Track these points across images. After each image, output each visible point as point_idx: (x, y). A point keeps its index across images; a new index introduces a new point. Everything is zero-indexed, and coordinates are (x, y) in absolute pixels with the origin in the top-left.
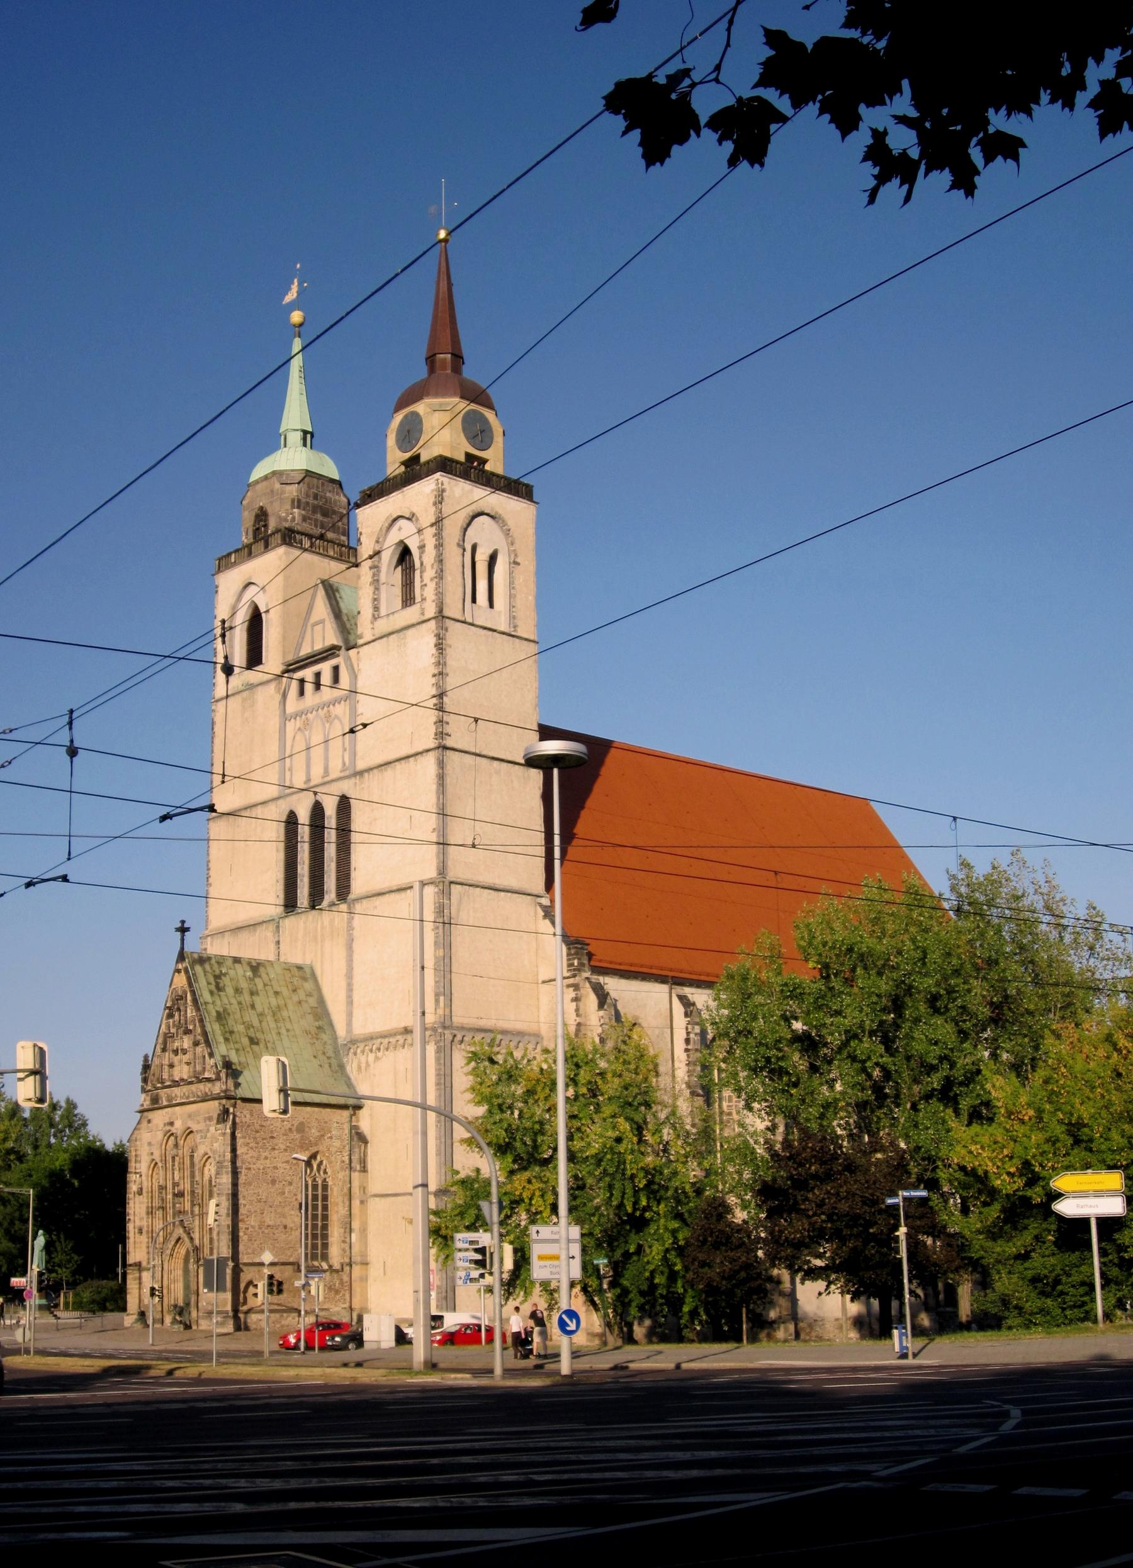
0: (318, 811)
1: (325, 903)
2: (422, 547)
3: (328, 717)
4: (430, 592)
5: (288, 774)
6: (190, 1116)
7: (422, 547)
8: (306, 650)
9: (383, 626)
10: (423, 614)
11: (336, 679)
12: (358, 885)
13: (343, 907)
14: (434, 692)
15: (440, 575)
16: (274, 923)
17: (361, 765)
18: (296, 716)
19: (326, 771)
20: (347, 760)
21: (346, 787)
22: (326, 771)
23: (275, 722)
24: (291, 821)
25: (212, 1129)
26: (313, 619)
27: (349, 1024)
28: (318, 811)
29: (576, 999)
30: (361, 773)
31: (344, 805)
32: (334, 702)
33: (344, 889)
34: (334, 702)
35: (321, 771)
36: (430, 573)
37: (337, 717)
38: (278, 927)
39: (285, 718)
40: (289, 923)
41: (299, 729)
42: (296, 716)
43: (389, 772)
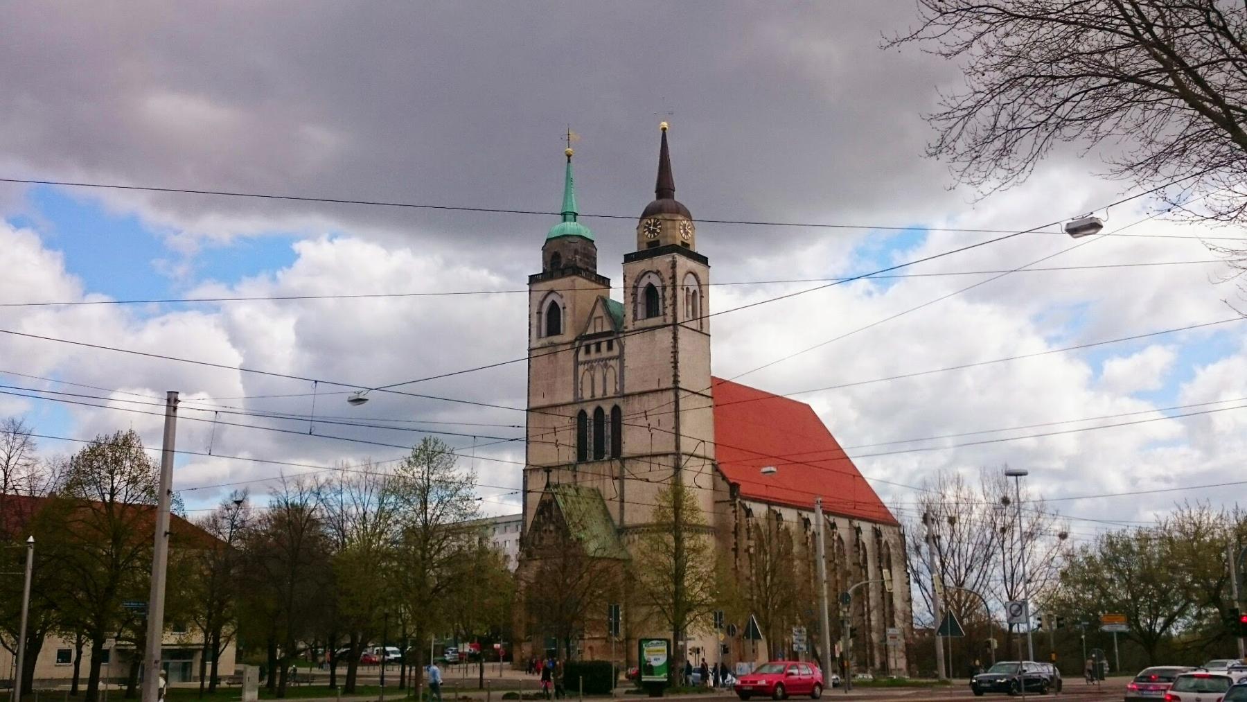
0: (599, 411)
1: (605, 458)
2: (664, 288)
3: (606, 366)
4: (669, 311)
8: (590, 331)
9: (639, 324)
11: (610, 348)
12: (627, 450)
13: (617, 463)
15: (674, 304)
16: (572, 467)
17: (627, 391)
18: (585, 363)
19: (605, 391)
22: (605, 391)
23: (571, 364)
24: (582, 414)
26: (596, 314)
27: (622, 520)
28: (599, 411)
29: (735, 512)
30: (628, 395)
31: (616, 410)
32: (610, 359)
34: (610, 359)
36: (668, 302)
38: (575, 470)
39: (577, 364)
40: (582, 467)
42: (585, 363)
43: (645, 398)
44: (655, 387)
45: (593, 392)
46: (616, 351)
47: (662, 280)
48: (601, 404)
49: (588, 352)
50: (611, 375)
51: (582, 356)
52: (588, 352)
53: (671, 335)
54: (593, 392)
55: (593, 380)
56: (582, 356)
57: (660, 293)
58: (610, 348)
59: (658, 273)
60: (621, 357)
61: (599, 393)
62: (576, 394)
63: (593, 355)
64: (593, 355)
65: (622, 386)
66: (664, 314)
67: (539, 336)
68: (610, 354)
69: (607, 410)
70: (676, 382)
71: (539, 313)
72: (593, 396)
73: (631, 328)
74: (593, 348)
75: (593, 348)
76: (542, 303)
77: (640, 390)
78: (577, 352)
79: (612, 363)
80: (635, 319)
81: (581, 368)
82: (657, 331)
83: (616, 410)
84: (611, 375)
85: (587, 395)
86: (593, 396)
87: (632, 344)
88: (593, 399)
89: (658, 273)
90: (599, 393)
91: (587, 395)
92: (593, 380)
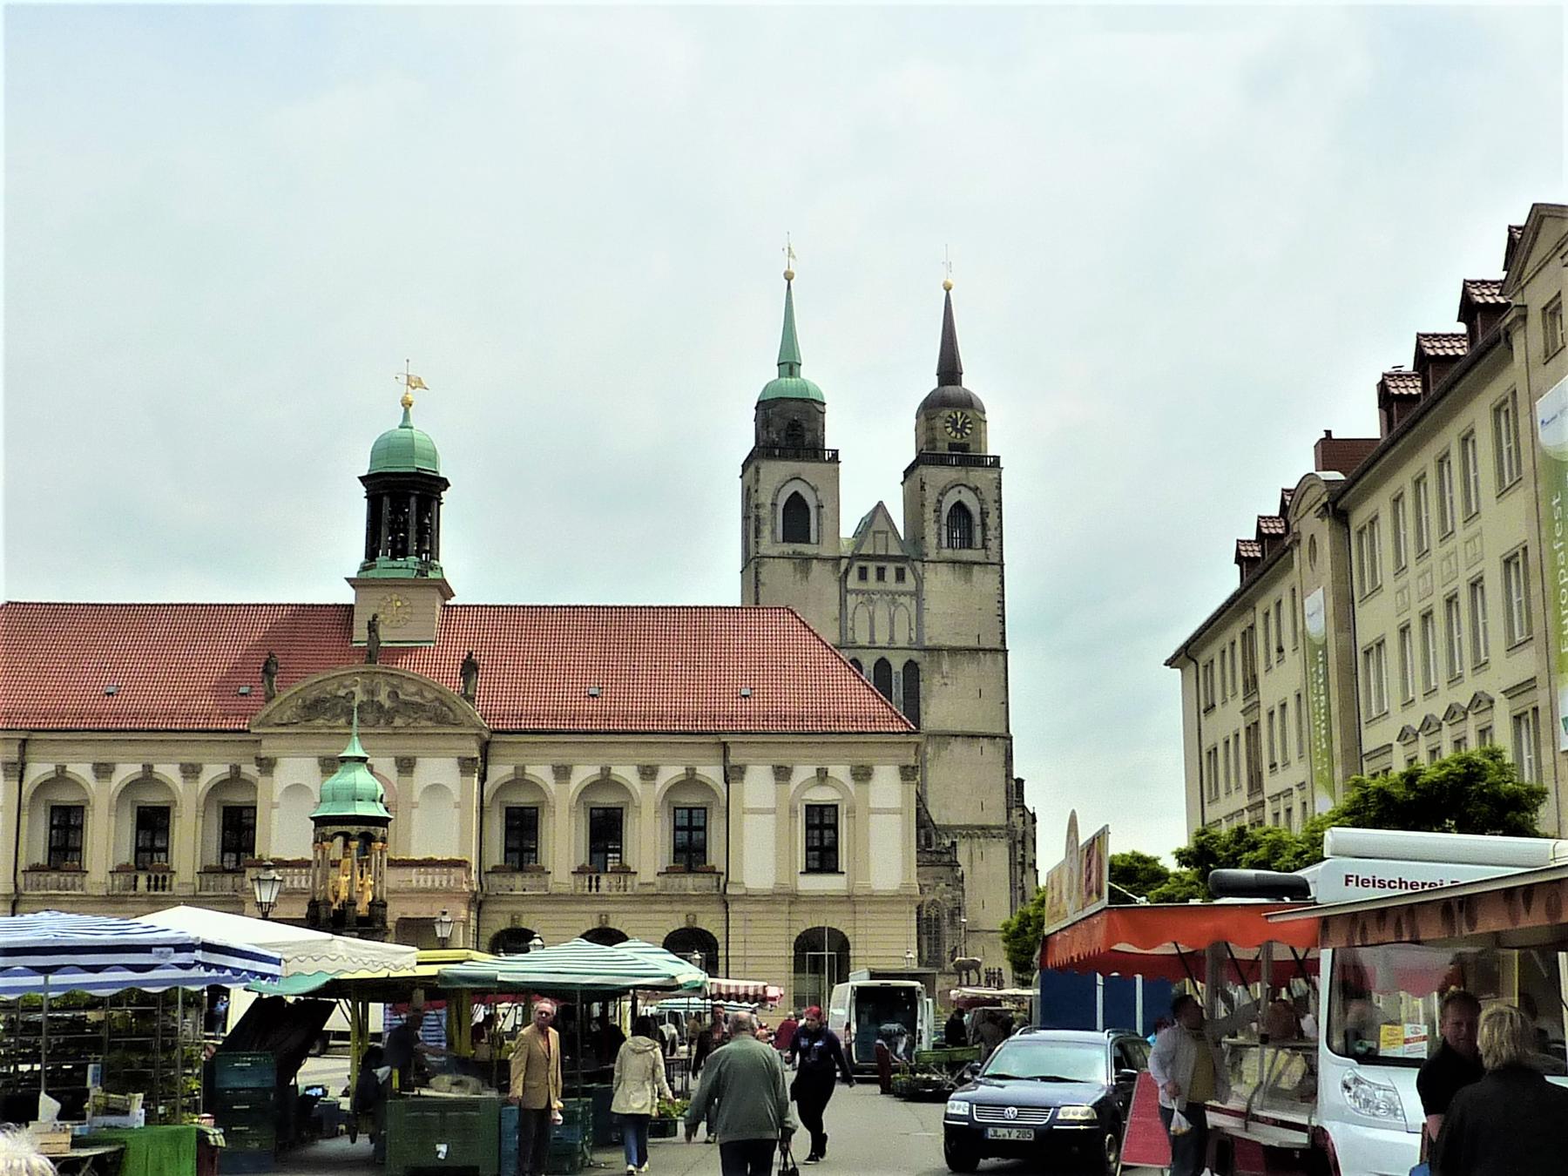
3: (894, 602)
7: (984, 514)
9: (947, 553)
11: (900, 576)
18: (857, 592)
19: (892, 638)
20: (913, 636)
21: (915, 656)
22: (892, 638)
23: (833, 590)
25: (942, 885)
26: (874, 528)
31: (911, 668)
39: (844, 592)
42: (857, 592)
44: (973, 643)
45: (872, 635)
46: (910, 583)
47: (982, 501)
48: (886, 654)
50: (902, 617)
51: (853, 582)
54: (872, 635)
55: (872, 619)
56: (853, 582)
57: (977, 519)
58: (900, 576)
59: (975, 490)
60: (917, 595)
62: (842, 631)
63: (872, 582)
64: (872, 582)
66: (985, 547)
68: (901, 587)
69: (897, 664)
70: (1003, 641)
71: (774, 505)
72: (872, 641)
73: (932, 555)
74: (872, 574)
75: (872, 574)
78: (847, 572)
79: (902, 599)
81: (851, 599)
82: (976, 567)
86: (872, 641)
87: (938, 581)
88: (872, 647)
89: (975, 490)
91: (863, 639)
92: (872, 619)
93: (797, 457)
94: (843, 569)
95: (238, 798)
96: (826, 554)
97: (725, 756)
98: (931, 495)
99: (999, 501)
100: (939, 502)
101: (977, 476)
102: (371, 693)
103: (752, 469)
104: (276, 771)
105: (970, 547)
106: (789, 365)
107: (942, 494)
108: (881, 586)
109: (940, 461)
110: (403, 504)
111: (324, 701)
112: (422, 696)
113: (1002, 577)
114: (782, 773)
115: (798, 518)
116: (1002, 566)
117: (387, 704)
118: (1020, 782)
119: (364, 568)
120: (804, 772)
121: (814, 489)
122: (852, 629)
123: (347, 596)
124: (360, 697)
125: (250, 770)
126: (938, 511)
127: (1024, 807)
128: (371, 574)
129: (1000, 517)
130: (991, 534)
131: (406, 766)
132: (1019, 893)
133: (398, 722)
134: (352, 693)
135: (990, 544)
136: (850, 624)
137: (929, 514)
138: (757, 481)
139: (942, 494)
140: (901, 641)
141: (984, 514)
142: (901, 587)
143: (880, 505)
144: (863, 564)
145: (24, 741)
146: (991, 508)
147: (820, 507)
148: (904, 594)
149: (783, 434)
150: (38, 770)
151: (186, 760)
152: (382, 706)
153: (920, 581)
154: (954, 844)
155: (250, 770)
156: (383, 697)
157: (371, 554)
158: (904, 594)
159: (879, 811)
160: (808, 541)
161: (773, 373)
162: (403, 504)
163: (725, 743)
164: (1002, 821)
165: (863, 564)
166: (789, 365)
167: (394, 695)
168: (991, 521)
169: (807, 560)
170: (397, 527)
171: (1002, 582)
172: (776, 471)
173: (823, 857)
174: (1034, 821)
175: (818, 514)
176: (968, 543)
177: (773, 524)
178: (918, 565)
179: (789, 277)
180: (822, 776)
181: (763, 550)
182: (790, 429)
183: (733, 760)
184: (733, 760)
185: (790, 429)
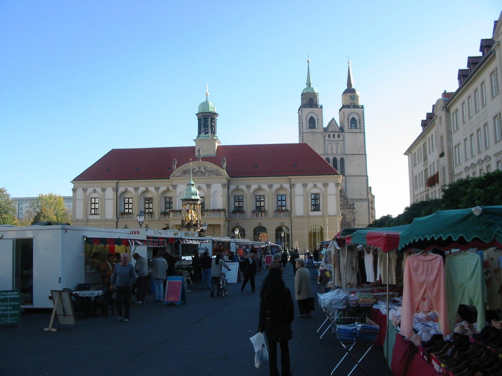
0: (335, 160)
5: (326, 151)
6: (344, 211)
7: (360, 120)
10: (361, 131)
11: (339, 136)
12: (347, 173)
14: (364, 145)
17: (346, 153)
18: (328, 141)
19: (337, 152)
21: (343, 156)
22: (337, 152)
23: (322, 141)
25: (351, 214)
33: (343, 173)
35: (336, 152)
37: (339, 143)
39: (325, 140)
41: (329, 143)
42: (328, 141)
47: (359, 117)
49: (329, 136)
51: (327, 138)
52: (329, 136)
53: (364, 136)
57: (358, 121)
58: (339, 136)
59: (357, 114)
60: (343, 141)
61: (334, 152)
62: (325, 151)
65: (344, 151)
66: (360, 128)
67: (307, 128)
70: (365, 152)
71: (306, 119)
72: (332, 153)
74: (332, 136)
75: (332, 136)
76: (307, 116)
77: (352, 153)
78: (325, 136)
79: (340, 142)
80: (349, 129)
81: (326, 143)
83: (342, 160)
84: (339, 147)
85: (330, 152)
86: (332, 153)
87: (348, 137)
88: (332, 154)
89: (357, 114)
90: (334, 152)
91: (330, 152)
92: (332, 147)
93: (312, 107)
94: (324, 135)
95: (169, 195)
96: (320, 131)
97: (290, 181)
98: (346, 116)
99: (363, 117)
100: (348, 117)
101: (357, 110)
102: (199, 168)
103: (300, 111)
104: (177, 188)
105: (356, 128)
106: (309, 84)
107: (349, 115)
108: (334, 139)
109: (348, 107)
110: (207, 121)
111: (188, 170)
112: (212, 169)
113: (365, 136)
114: (305, 185)
115: (312, 123)
116: (364, 133)
117: (203, 171)
118: (370, 188)
119: (198, 137)
120: (310, 185)
121: (317, 115)
122: (327, 150)
123: (193, 144)
124: (197, 169)
125: (171, 188)
126: (348, 119)
127: (371, 194)
128: (200, 138)
129: (364, 120)
130: (362, 125)
131: (209, 186)
132: (371, 215)
133: (206, 175)
134: (194, 168)
135: (361, 128)
136: (326, 149)
137: (346, 121)
138: (302, 114)
139: (349, 115)
140: (340, 152)
141: (360, 120)
142: (339, 139)
143: (333, 119)
144: (329, 133)
145: (117, 182)
146: (362, 118)
147: (318, 119)
148: (340, 141)
149: (308, 102)
150: (121, 189)
151: (156, 186)
152: (202, 172)
153: (344, 137)
154: (354, 203)
155: (171, 188)
156: (202, 169)
157: (199, 133)
158: (340, 141)
159: (330, 195)
160: (315, 128)
161: (305, 86)
162: (207, 121)
163: (290, 178)
164: (366, 197)
165: (329, 133)
166: (309, 84)
167: (205, 168)
168: (362, 122)
169: (315, 133)
170: (206, 126)
171: (365, 137)
172: (307, 111)
173: (316, 207)
174: (374, 197)
175: (318, 121)
176: (356, 128)
177: (306, 124)
178: (343, 133)
179: (308, 62)
180: (315, 186)
181: (305, 131)
182: (310, 101)
183: (292, 183)
184: (292, 183)
185: (310, 101)
